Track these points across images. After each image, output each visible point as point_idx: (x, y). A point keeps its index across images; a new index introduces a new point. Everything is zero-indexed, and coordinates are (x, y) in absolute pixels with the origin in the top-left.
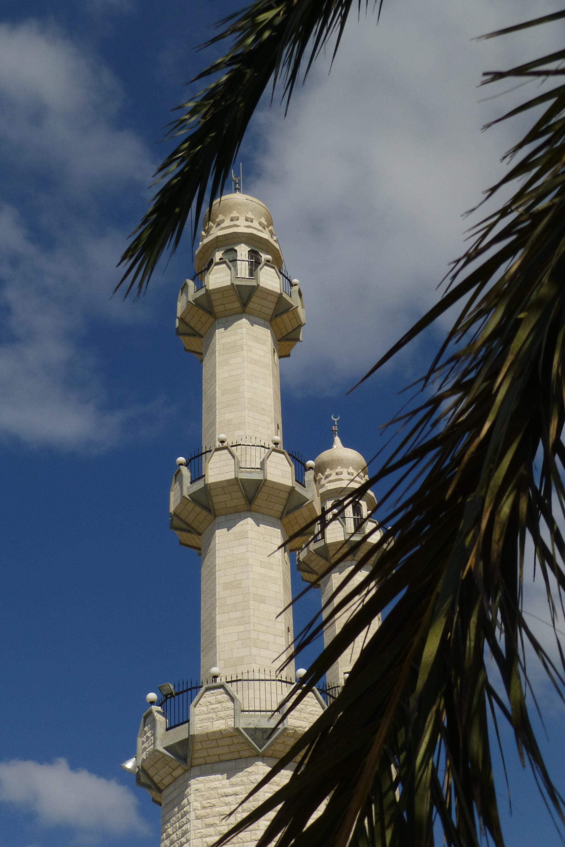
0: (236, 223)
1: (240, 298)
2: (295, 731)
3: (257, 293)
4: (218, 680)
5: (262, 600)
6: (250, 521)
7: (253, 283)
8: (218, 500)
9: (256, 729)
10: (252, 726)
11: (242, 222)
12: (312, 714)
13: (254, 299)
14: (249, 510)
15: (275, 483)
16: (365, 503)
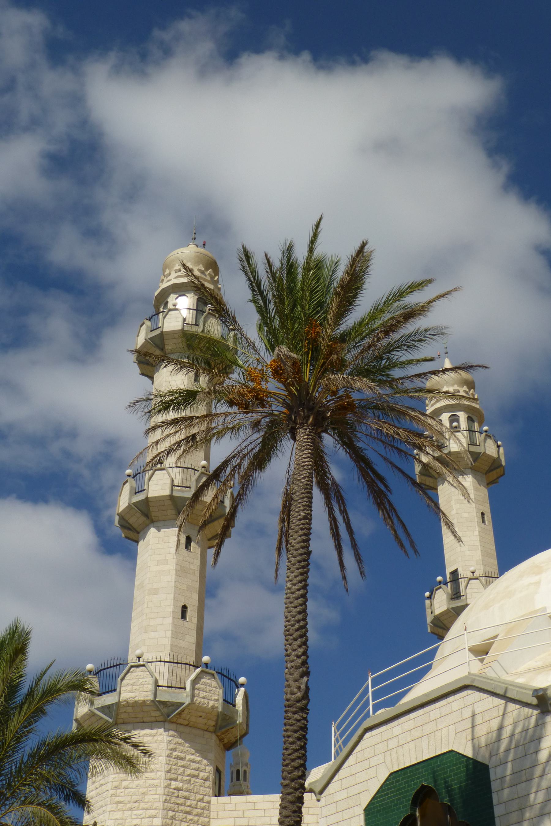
0: (169, 278)
1: (157, 346)
2: (128, 702)
3: (165, 337)
4: (141, 660)
5: (155, 592)
6: (153, 530)
7: (158, 332)
8: (132, 521)
9: (103, 707)
10: (100, 706)
11: (173, 275)
12: (143, 685)
13: (166, 342)
14: (152, 522)
15: (155, 497)
16: (463, 413)
